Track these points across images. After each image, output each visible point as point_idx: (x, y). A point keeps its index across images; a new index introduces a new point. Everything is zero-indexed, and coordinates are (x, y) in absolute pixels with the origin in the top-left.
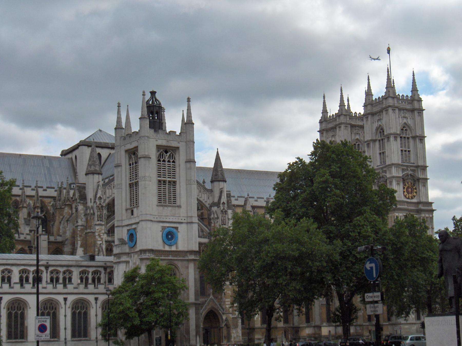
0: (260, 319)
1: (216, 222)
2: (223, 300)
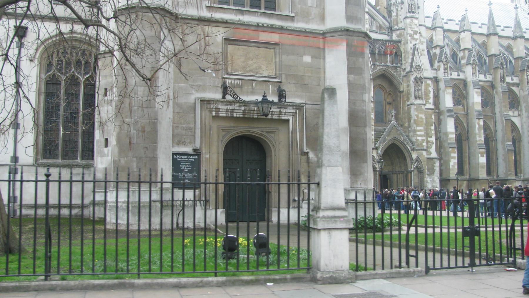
0: (456, 167)
1: (399, 9)
2: (413, 128)
